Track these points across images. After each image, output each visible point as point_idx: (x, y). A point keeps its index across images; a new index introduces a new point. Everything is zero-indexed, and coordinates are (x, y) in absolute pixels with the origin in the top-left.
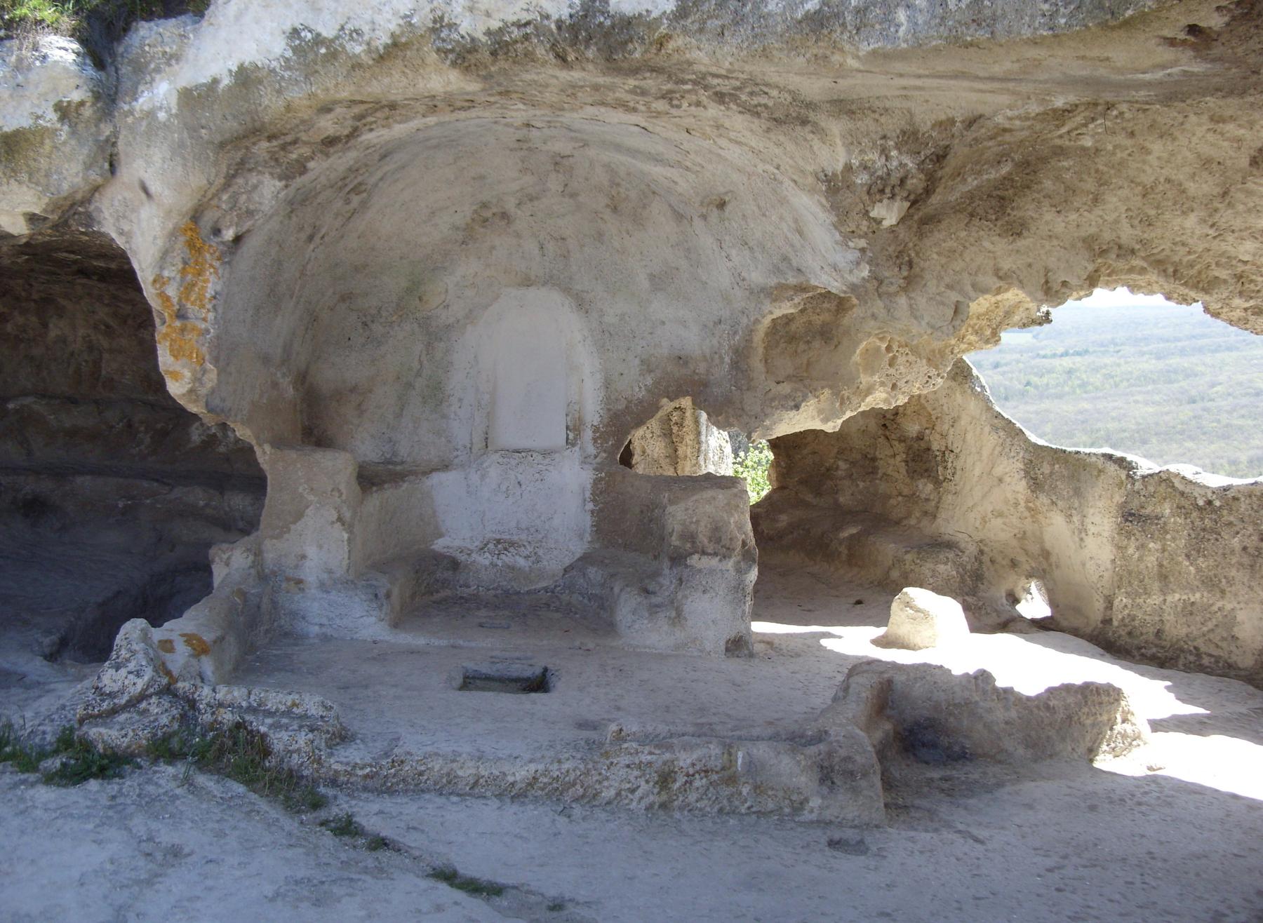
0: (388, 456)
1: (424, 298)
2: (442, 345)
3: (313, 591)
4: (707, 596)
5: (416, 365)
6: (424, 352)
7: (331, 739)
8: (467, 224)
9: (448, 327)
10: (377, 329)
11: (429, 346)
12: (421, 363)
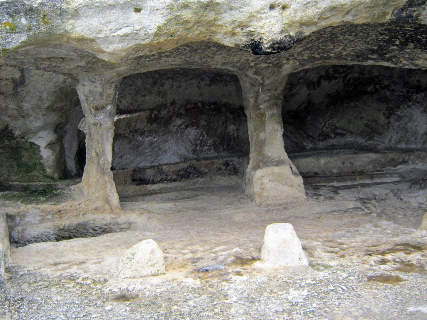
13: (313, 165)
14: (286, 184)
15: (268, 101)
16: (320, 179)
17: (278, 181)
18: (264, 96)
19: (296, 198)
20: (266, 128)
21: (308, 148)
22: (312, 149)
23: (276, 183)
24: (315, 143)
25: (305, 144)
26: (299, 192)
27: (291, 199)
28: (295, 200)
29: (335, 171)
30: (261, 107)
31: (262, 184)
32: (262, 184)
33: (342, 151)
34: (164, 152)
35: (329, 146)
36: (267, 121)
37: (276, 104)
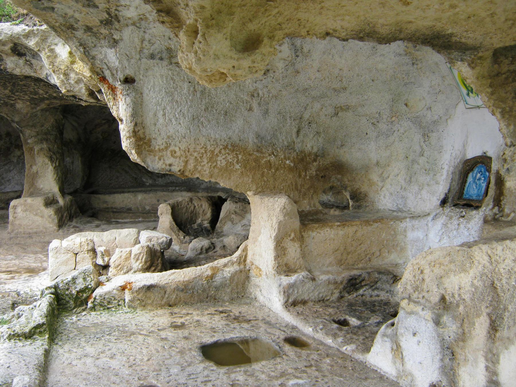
0: (400, 207)
1: (409, 104)
2: (434, 134)
3: (264, 277)
4: (416, 339)
5: (417, 148)
6: (422, 140)
7: (14, 335)
8: (405, 51)
9: (435, 123)
10: (383, 126)
11: (426, 136)
12: (421, 147)
13: (129, 201)
14: (36, 215)
15: (35, 136)
16: (127, 215)
17: (30, 212)
18: (30, 131)
19: (46, 228)
20: (37, 162)
21: (148, 184)
22: (151, 185)
23: (28, 213)
24: (155, 180)
25: (144, 180)
26: (49, 222)
27: (41, 229)
28: (44, 230)
29: (148, 208)
30: (29, 141)
31: (14, 213)
32: (14, 213)
33: (177, 188)
34: (8, 181)
35: (168, 183)
36: (36, 155)
37: (47, 140)
